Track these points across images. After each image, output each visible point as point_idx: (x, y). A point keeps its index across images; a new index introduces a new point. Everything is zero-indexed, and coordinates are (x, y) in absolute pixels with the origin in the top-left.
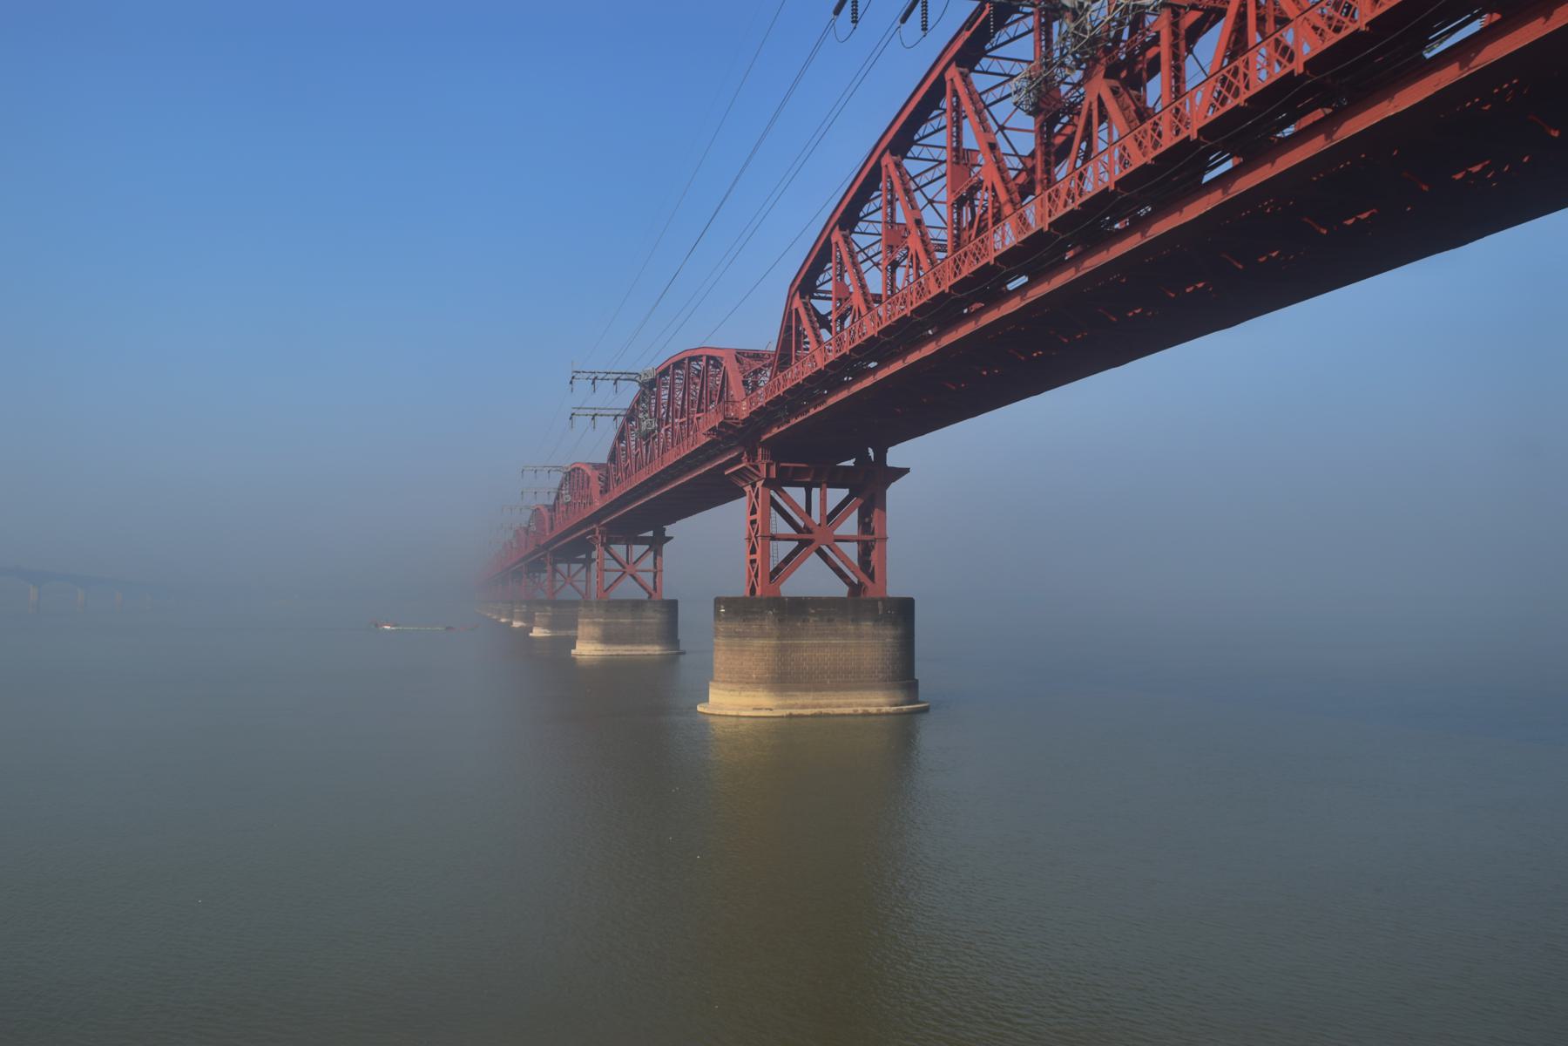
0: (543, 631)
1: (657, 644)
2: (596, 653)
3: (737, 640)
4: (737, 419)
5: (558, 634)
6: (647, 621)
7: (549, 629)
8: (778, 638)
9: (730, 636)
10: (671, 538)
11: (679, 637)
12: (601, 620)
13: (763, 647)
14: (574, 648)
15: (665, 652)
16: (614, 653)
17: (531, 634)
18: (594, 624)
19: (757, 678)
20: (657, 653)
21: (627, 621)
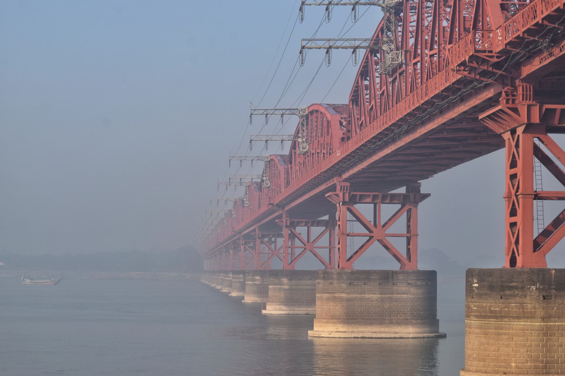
0: (278, 307)
1: (412, 324)
2: (337, 335)
3: (492, 321)
4: (491, 52)
5: (296, 312)
7: (286, 305)
8: (543, 319)
9: (485, 317)
10: (427, 196)
11: (438, 318)
12: (344, 295)
13: (522, 330)
14: (312, 328)
15: (422, 335)
16: (360, 335)
18: (335, 299)
19: (516, 366)
20: (411, 336)
21: (375, 296)
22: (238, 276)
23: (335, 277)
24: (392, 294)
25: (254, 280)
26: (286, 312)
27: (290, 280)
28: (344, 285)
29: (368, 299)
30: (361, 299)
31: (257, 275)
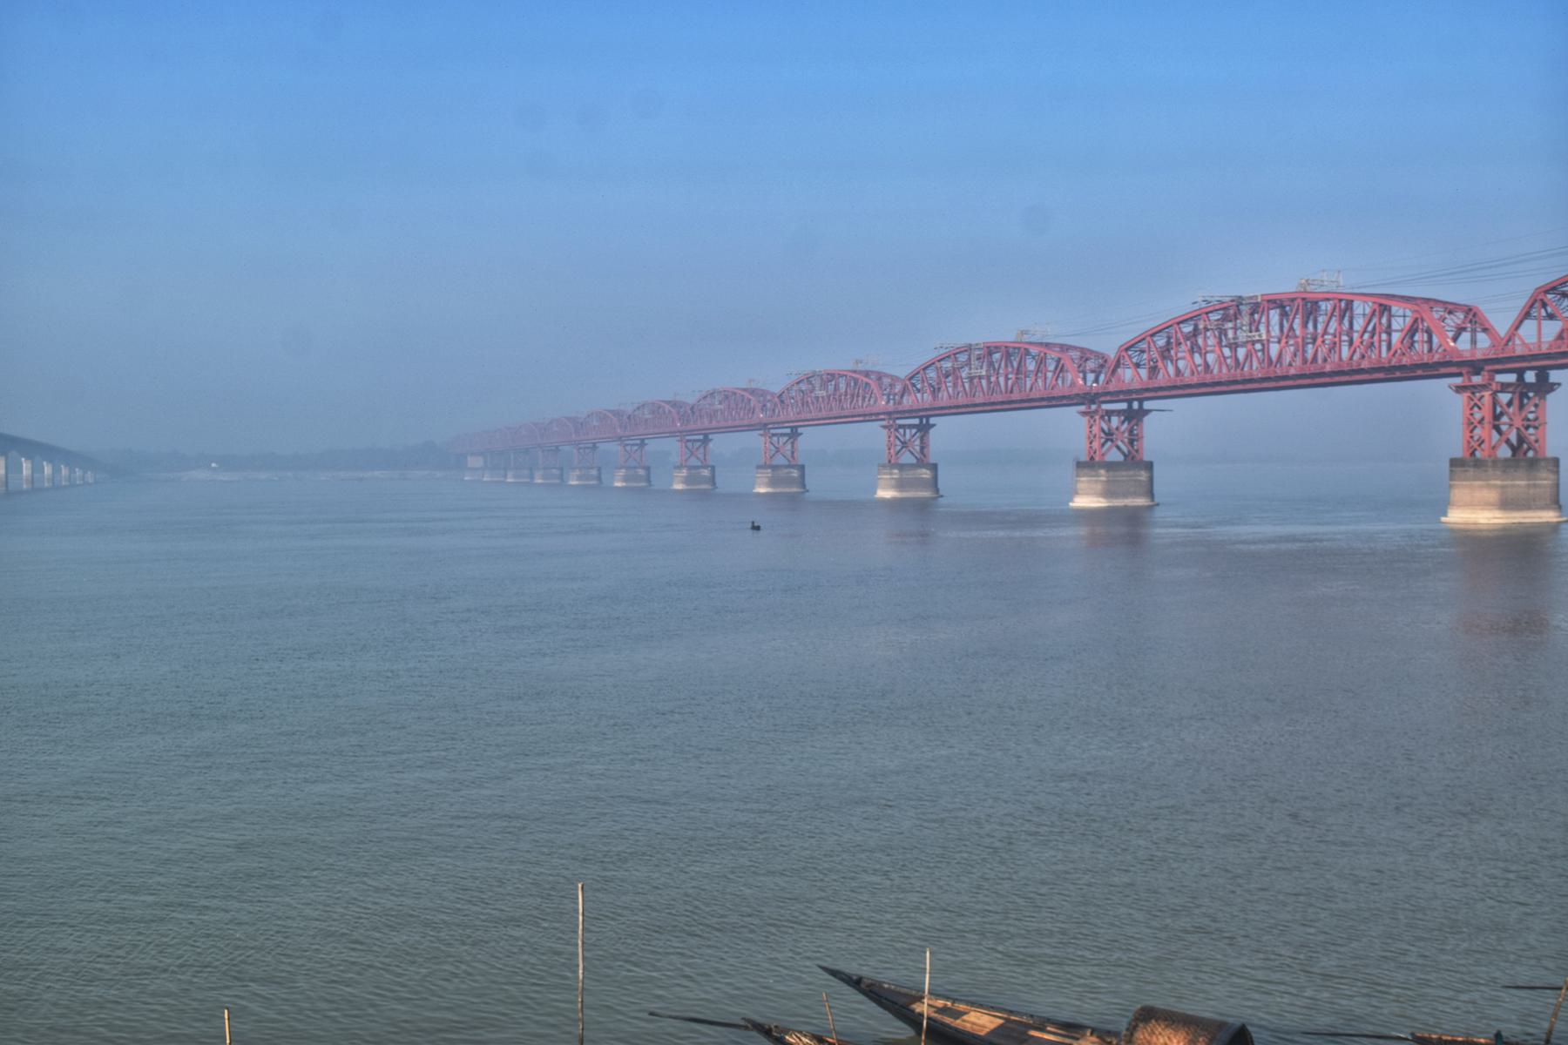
0: (1096, 499)
5: (1116, 504)
6: (1540, 482)
12: (1499, 482)
17: (1071, 504)
18: (1489, 487)
21: (1523, 483)
22: (765, 471)
23: (1490, 464)
24: (1536, 479)
25: (891, 474)
26: (1106, 505)
27: (1108, 471)
28: (1499, 473)
29: (1518, 485)
30: (1513, 486)
31: (895, 468)
